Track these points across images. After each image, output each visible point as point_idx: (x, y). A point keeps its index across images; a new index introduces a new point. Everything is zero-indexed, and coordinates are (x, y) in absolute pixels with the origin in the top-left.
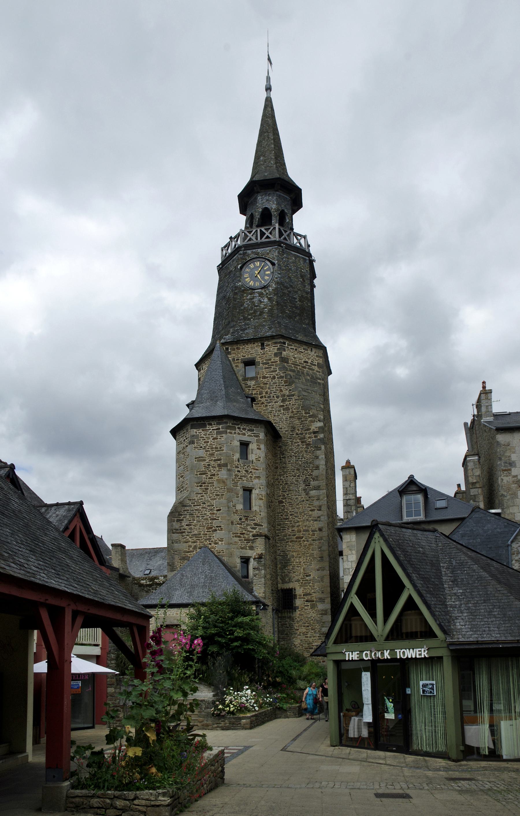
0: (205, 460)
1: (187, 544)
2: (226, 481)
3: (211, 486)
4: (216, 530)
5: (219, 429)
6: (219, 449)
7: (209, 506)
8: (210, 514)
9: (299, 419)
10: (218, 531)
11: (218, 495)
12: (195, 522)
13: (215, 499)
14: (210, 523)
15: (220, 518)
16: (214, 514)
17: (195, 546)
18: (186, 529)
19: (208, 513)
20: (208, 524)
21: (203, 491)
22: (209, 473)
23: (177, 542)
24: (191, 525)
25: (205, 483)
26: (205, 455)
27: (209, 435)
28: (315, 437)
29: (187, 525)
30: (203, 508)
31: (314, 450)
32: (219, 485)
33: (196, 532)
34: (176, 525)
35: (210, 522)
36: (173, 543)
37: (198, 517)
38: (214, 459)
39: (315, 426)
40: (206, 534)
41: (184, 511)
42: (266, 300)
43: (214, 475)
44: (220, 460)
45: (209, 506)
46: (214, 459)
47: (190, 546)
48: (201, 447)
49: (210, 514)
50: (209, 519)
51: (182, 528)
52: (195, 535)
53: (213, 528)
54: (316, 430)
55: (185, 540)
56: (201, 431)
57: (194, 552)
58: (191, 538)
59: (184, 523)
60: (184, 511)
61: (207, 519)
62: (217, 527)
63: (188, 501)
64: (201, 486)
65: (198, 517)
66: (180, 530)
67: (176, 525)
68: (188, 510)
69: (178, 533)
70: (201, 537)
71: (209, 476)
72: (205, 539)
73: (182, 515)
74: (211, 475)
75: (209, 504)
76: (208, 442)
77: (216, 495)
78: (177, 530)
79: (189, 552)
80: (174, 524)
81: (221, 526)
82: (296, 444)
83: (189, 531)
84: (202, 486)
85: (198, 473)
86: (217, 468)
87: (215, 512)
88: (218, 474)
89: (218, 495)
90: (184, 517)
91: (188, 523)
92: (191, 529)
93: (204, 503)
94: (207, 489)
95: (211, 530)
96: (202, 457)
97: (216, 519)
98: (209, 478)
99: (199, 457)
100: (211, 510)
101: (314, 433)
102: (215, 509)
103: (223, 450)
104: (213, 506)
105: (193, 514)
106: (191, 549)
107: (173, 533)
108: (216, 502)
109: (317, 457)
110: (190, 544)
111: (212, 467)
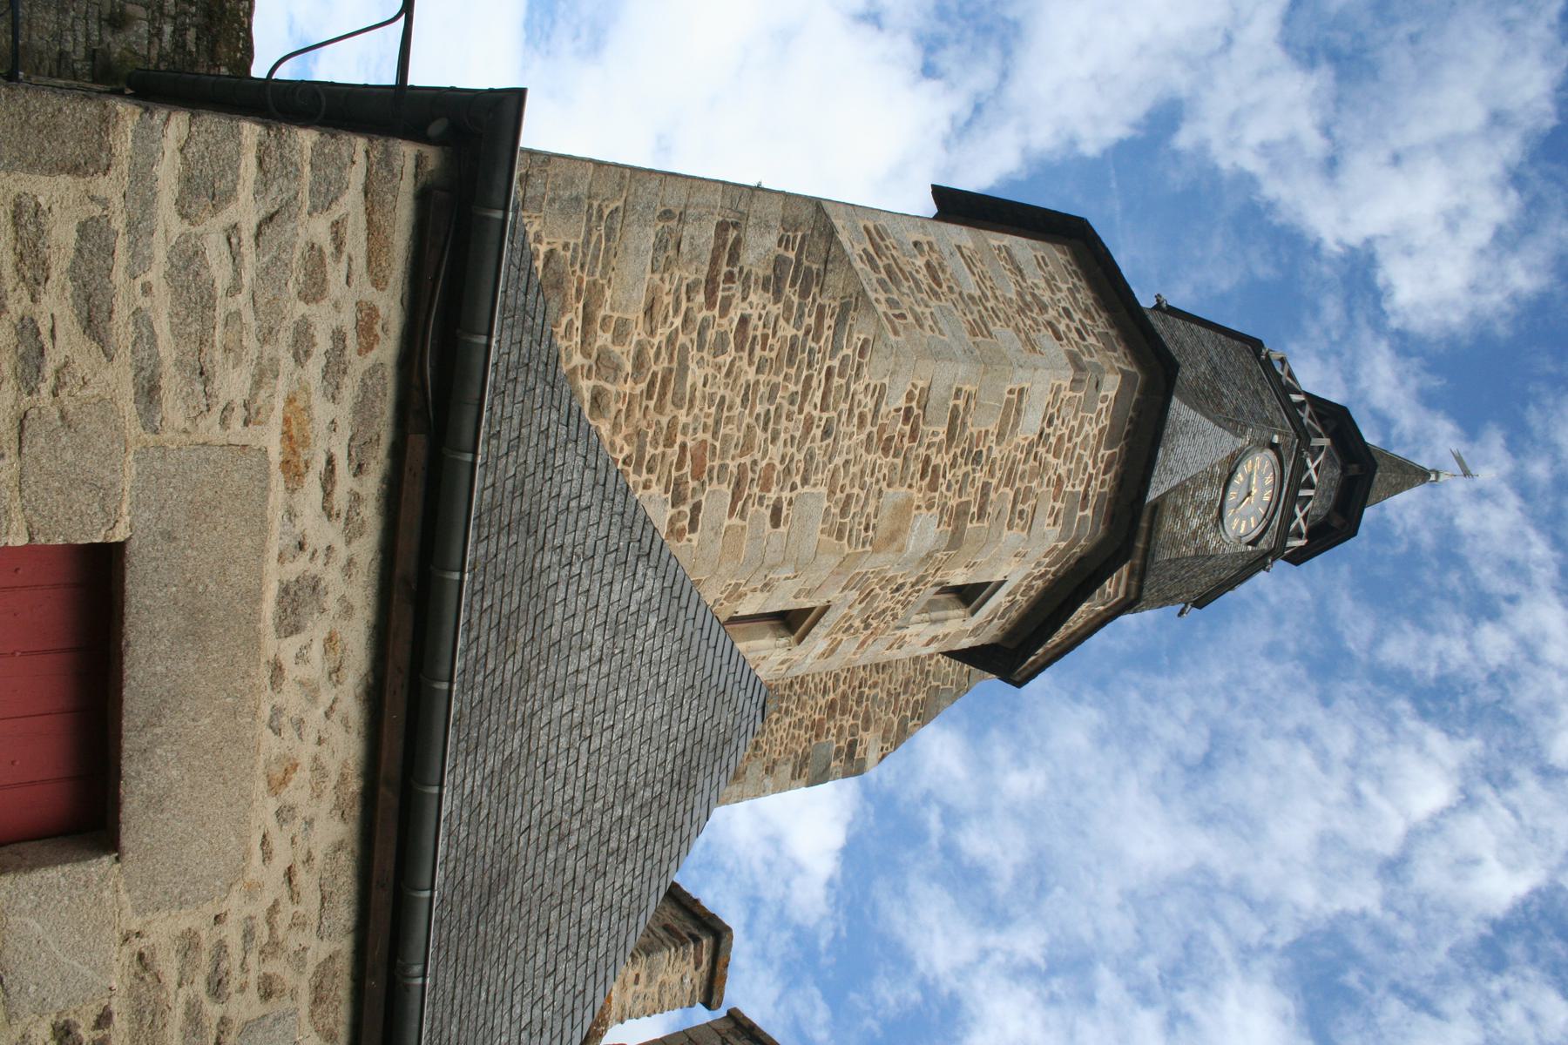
0: (1000, 436)
1: (636, 314)
2: (895, 546)
3: (893, 467)
4: (678, 500)
5: (1083, 508)
6: (1020, 507)
7: (810, 456)
8: (771, 466)
9: (907, 684)
10: (670, 512)
11: (843, 513)
12: (751, 375)
13: (832, 492)
14: (723, 467)
15: (736, 520)
16: (766, 487)
17: (617, 368)
18: (724, 312)
19: (775, 452)
20: (724, 452)
21: (882, 429)
22: (947, 459)
23: (661, 245)
24: (740, 347)
25: (913, 437)
26: (1019, 439)
27: (1080, 457)
28: (839, 750)
29: (744, 320)
30: (809, 423)
31: (796, 756)
32: (886, 512)
33: (695, 374)
34: (759, 249)
35: (732, 466)
36: (666, 215)
37: (774, 389)
38: (994, 482)
39: (871, 747)
40: (669, 443)
41: (821, 309)
42: (1195, 523)
43: (933, 487)
44: (981, 514)
45: (810, 456)
46: (994, 482)
47: (621, 333)
48: (1050, 423)
49: (771, 466)
50: (747, 460)
51: (737, 287)
52: (684, 368)
53: (692, 484)
54: (858, 748)
55: (668, 299)
56: (1105, 421)
57: (578, 359)
58: (671, 340)
59: (757, 304)
60: (821, 309)
61: (747, 447)
62: (697, 508)
63: (858, 338)
64: (908, 410)
65: (774, 389)
66: (730, 277)
67: (759, 249)
68: (817, 339)
69: (714, 261)
70: (660, 408)
71: (935, 460)
72: (640, 434)
73: (804, 294)
74: (935, 469)
75: (819, 458)
76: (1056, 455)
77: (849, 497)
78: (734, 258)
79: (588, 319)
80: (771, 240)
81: (693, 526)
82: (830, 683)
83: (711, 335)
84: (906, 420)
85: (961, 403)
86: (953, 503)
87: (772, 495)
88: (929, 507)
89: (843, 513)
90: (788, 307)
91: (756, 329)
92: (720, 347)
93: (826, 433)
94: (886, 451)
95: (687, 469)
96: (1016, 425)
97: (736, 497)
98: (927, 460)
99: (1018, 411)
100: (788, 471)
101: (852, 745)
102: (786, 494)
103: (1010, 527)
104: (805, 481)
105: (790, 362)
106: (603, 339)
107: (722, 227)
108: (818, 497)
109: (769, 770)
110: (637, 334)
111: (966, 475)
